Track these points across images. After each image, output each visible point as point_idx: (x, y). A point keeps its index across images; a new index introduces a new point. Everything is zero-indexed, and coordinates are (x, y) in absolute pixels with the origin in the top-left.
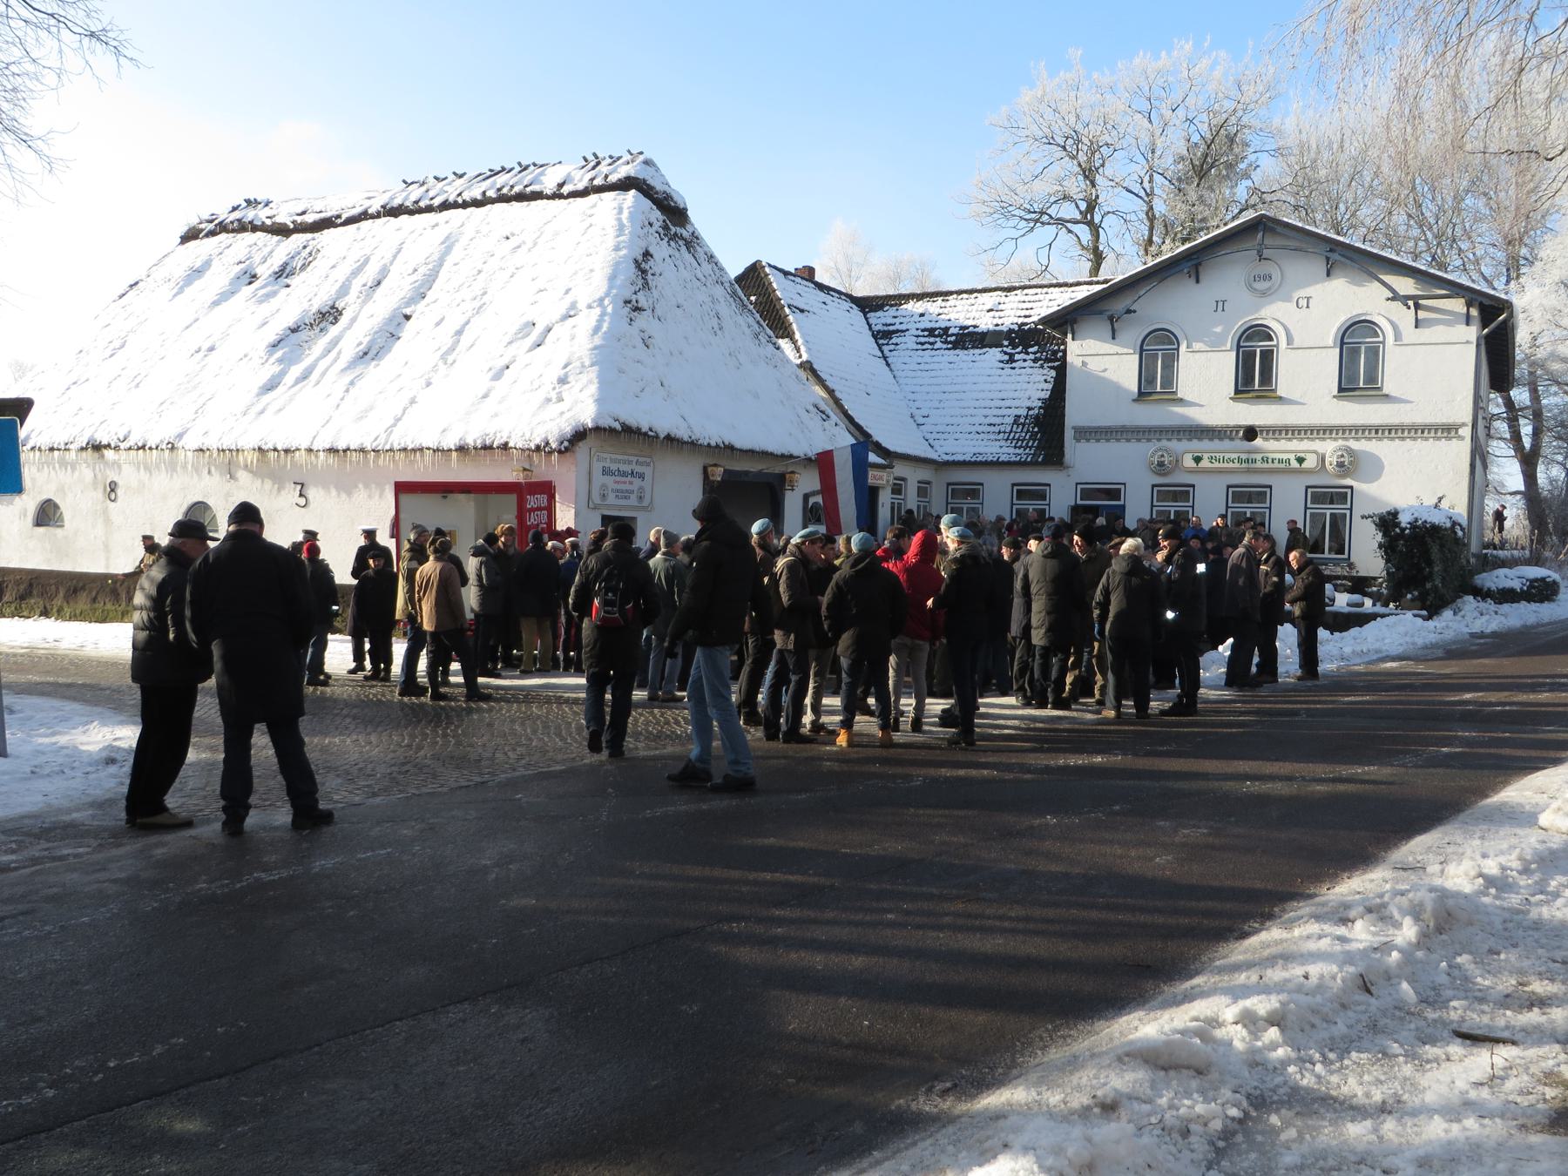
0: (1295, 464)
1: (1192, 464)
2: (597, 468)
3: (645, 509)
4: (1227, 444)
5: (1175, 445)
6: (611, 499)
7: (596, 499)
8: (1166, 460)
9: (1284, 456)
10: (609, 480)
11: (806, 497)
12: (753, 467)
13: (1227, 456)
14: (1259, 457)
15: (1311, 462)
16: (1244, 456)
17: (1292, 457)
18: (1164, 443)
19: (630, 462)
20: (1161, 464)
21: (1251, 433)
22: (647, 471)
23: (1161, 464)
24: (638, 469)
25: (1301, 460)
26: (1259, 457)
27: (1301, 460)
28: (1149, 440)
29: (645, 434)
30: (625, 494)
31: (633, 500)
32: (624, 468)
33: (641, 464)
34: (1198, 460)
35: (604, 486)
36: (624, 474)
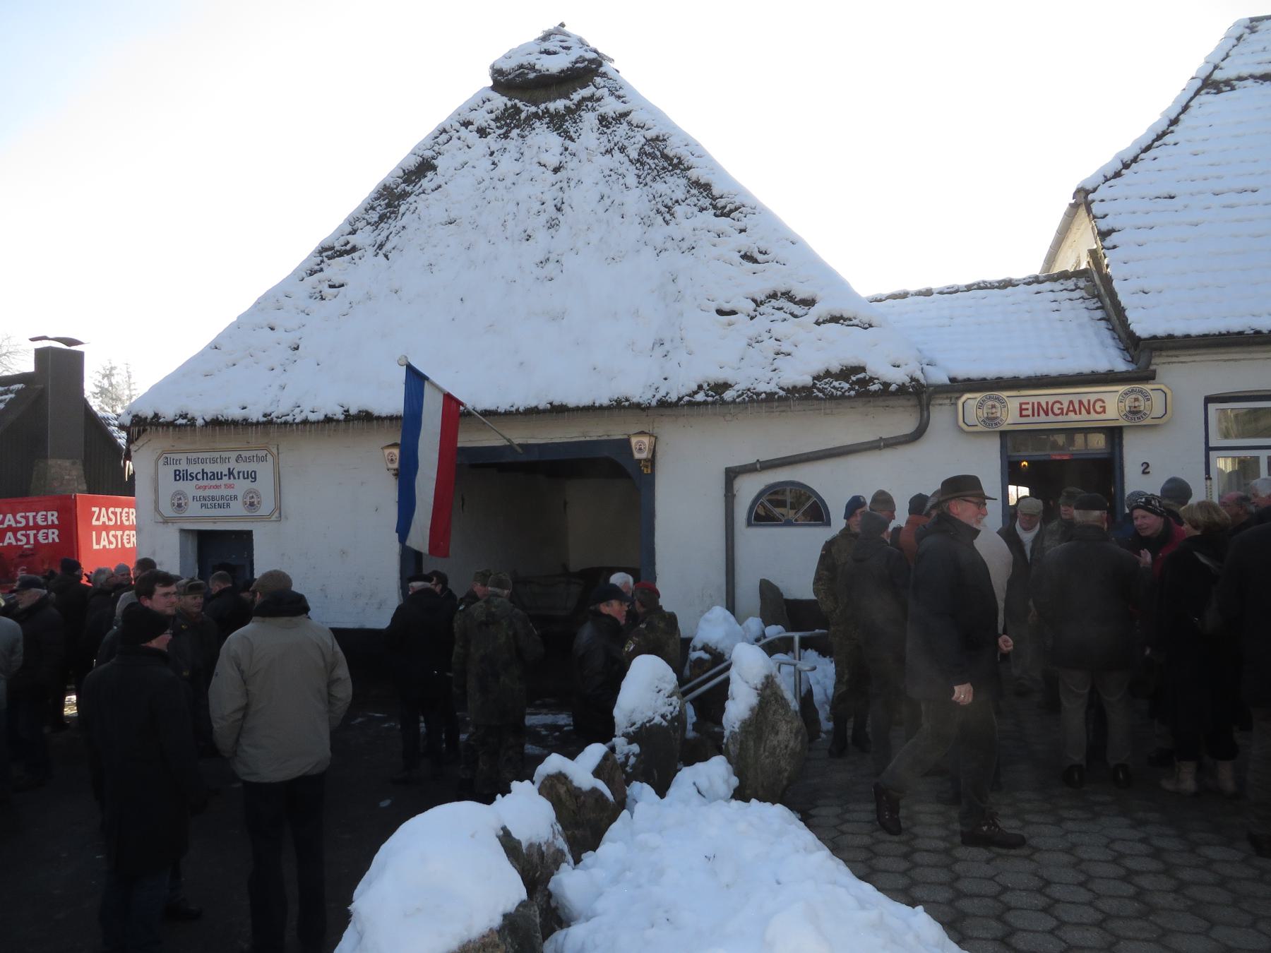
2: (167, 472)
3: (262, 518)
6: (194, 509)
7: (168, 511)
10: (189, 487)
11: (732, 475)
12: (521, 436)
19: (223, 460)
22: (265, 471)
24: (238, 467)
29: (171, 424)
30: (224, 502)
31: (237, 508)
32: (209, 468)
33: (250, 459)
35: (179, 495)
36: (215, 476)
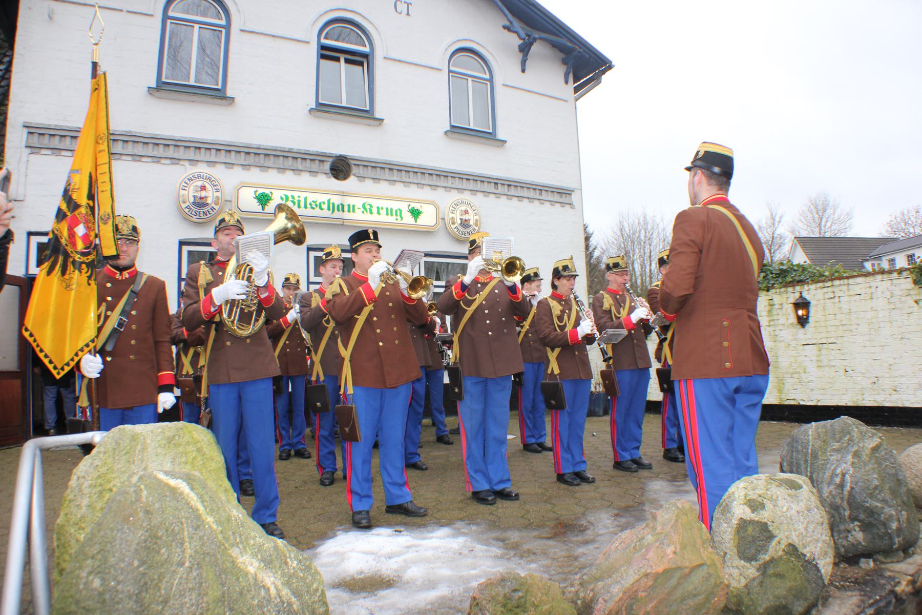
0: (408, 219)
1: (256, 206)
4: (305, 180)
5: (219, 172)
8: (210, 195)
9: (395, 205)
13: (311, 197)
14: (358, 202)
15: (428, 218)
16: (336, 200)
17: (404, 207)
18: (202, 169)
20: (200, 203)
21: (340, 168)
23: (200, 203)
25: (415, 213)
26: (358, 202)
27: (415, 213)
28: (175, 160)
34: (264, 200)
